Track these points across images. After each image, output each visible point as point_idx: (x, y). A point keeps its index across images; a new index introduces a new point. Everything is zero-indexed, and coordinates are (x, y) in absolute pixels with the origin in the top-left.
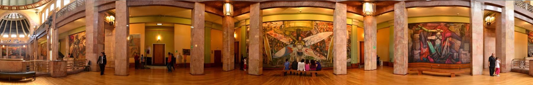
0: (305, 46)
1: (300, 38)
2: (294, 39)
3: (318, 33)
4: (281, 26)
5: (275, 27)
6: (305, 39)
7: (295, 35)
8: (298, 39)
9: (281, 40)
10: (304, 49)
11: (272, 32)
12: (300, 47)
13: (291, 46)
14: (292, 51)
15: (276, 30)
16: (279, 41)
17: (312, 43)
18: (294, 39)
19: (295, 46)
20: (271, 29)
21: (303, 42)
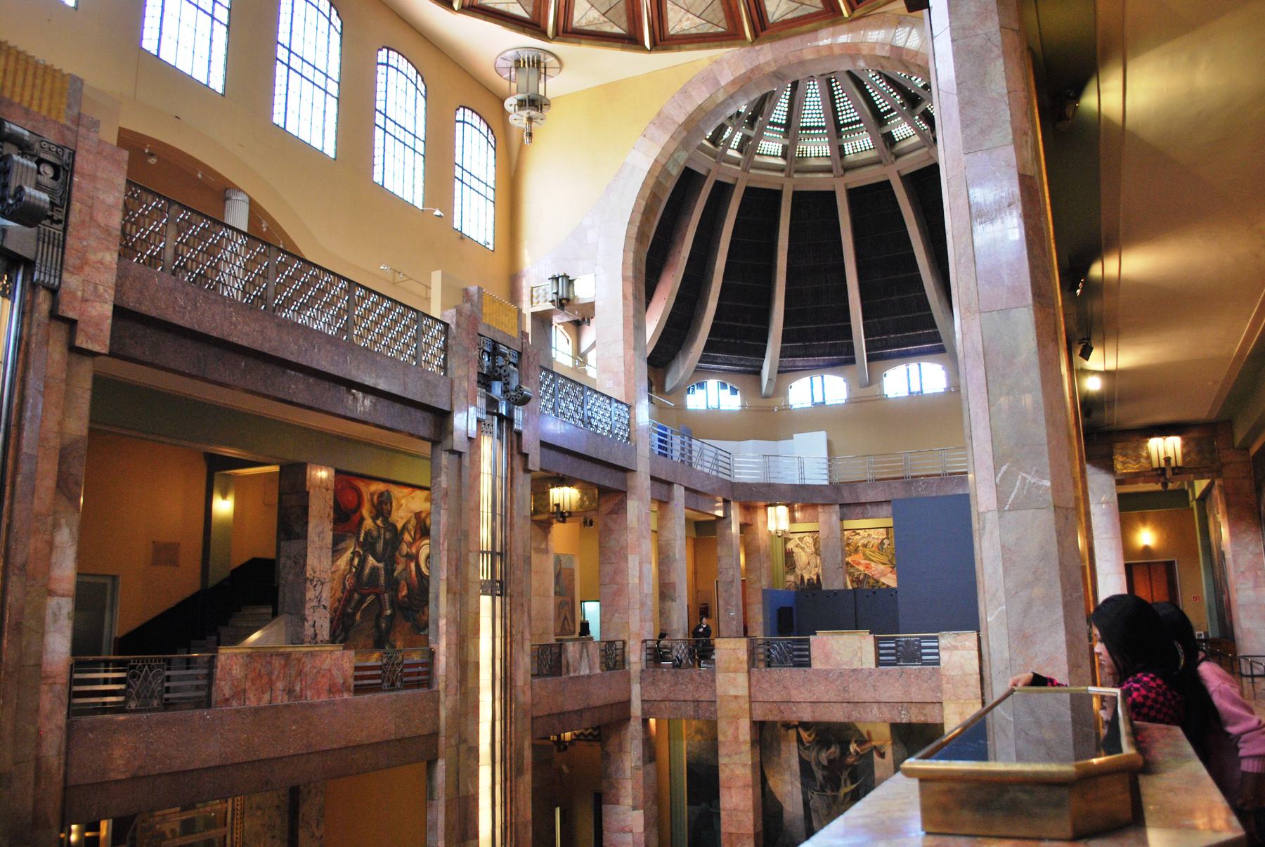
4: (882, 543)
5: (865, 546)
9: (883, 580)
11: (857, 558)
15: (868, 552)
16: (878, 582)
20: (856, 550)
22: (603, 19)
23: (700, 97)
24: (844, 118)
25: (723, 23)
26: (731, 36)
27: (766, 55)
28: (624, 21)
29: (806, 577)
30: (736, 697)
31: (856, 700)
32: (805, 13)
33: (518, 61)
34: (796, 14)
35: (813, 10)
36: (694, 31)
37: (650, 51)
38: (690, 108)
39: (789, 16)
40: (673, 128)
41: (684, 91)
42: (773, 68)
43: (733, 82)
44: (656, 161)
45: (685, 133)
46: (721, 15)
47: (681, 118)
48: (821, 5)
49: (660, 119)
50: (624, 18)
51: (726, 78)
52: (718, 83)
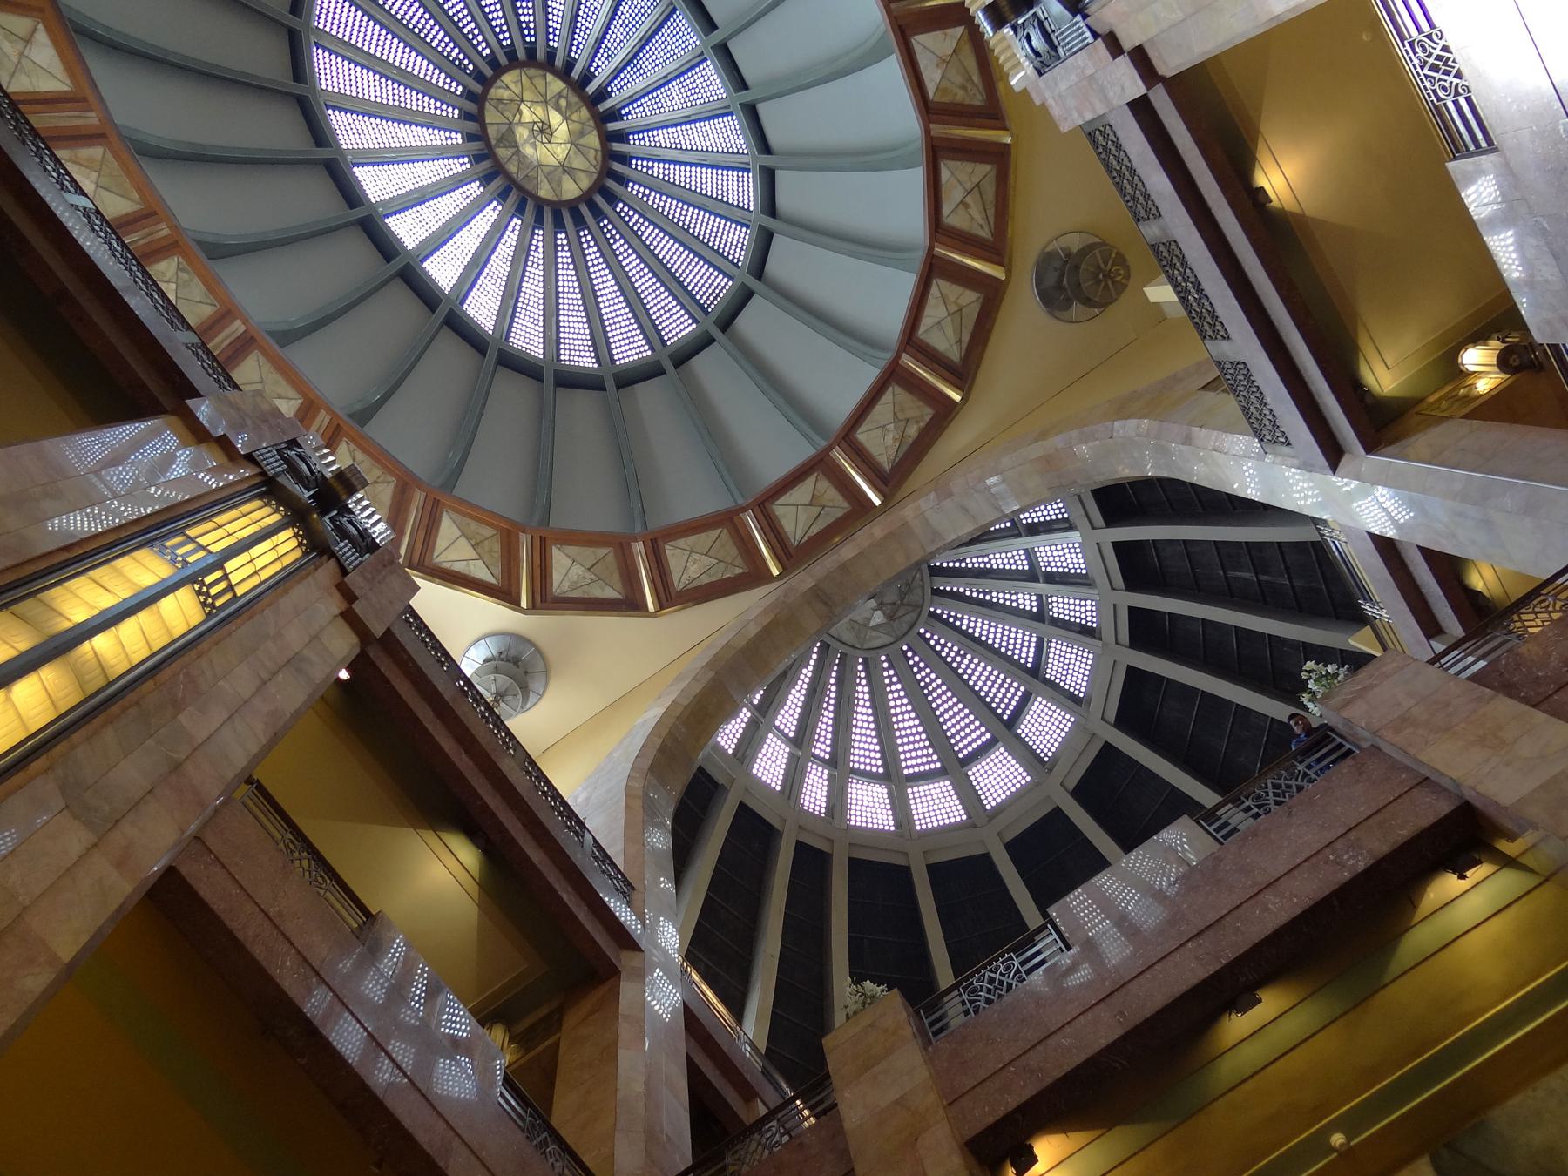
22: (589, 575)
24: (964, 747)
25: (739, 561)
26: (755, 575)
28: (616, 578)
30: (897, 1102)
31: (1212, 917)
32: (830, 520)
35: (839, 513)
36: (705, 580)
37: (654, 614)
39: (815, 530)
42: (810, 583)
45: (711, 674)
46: (734, 551)
48: (846, 505)
49: (679, 679)
50: (616, 576)
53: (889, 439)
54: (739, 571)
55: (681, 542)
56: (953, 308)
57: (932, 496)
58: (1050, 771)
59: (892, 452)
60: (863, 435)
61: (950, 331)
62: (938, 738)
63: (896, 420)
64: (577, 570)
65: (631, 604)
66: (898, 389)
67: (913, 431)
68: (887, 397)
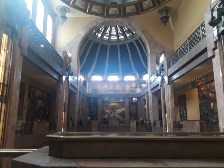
0: (116, 114)
1: (114, 110)
2: (112, 111)
3: (121, 108)
6: (116, 111)
7: (112, 109)
8: (113, 111)
9: (106, 111)
10: (116, 115)
12: (114, 114)
13: (110, 114)
14: (110, 116)
17: (119, 112)
18: (112, 111)
19: (112, 114)
21: (115, 112)
23: (94, 24)
27: (107, 20)
29: (93, 110)
33: (62, 8)
34: (114, 14)
36: (96, 12)
37: (87, 14)
38: (93, 26)
40: (89, 29)
41: (91, 22)
43: (101, 23)
44: (85, 34)
46: (101, 10)
47: (91, 27)
51: (100, 22)
52: (98, 22)
53: (129, 11)
54: (100, 13)
55: (95, 6)
56: (149, 4)
57: (128, 24)
58: (119, 42)
59: (128, 12)
60: (127, 8)
61: (146, 6)
62: (110, 31)
63: (131, 10)
64: (80, 4)
65: (84, 11)
66: (135, 6)
67: (132, 12)
68: (133, 6)
